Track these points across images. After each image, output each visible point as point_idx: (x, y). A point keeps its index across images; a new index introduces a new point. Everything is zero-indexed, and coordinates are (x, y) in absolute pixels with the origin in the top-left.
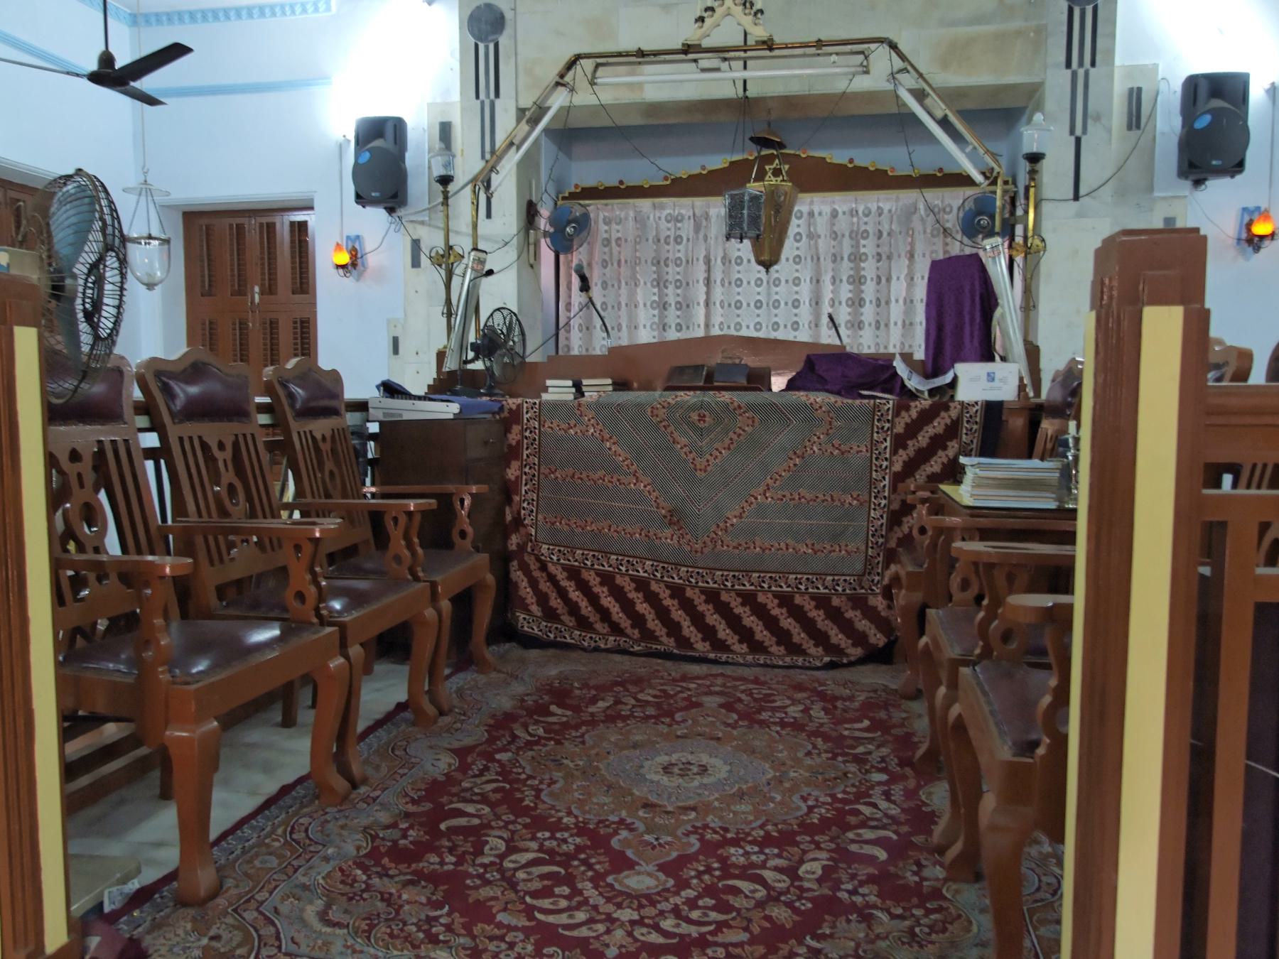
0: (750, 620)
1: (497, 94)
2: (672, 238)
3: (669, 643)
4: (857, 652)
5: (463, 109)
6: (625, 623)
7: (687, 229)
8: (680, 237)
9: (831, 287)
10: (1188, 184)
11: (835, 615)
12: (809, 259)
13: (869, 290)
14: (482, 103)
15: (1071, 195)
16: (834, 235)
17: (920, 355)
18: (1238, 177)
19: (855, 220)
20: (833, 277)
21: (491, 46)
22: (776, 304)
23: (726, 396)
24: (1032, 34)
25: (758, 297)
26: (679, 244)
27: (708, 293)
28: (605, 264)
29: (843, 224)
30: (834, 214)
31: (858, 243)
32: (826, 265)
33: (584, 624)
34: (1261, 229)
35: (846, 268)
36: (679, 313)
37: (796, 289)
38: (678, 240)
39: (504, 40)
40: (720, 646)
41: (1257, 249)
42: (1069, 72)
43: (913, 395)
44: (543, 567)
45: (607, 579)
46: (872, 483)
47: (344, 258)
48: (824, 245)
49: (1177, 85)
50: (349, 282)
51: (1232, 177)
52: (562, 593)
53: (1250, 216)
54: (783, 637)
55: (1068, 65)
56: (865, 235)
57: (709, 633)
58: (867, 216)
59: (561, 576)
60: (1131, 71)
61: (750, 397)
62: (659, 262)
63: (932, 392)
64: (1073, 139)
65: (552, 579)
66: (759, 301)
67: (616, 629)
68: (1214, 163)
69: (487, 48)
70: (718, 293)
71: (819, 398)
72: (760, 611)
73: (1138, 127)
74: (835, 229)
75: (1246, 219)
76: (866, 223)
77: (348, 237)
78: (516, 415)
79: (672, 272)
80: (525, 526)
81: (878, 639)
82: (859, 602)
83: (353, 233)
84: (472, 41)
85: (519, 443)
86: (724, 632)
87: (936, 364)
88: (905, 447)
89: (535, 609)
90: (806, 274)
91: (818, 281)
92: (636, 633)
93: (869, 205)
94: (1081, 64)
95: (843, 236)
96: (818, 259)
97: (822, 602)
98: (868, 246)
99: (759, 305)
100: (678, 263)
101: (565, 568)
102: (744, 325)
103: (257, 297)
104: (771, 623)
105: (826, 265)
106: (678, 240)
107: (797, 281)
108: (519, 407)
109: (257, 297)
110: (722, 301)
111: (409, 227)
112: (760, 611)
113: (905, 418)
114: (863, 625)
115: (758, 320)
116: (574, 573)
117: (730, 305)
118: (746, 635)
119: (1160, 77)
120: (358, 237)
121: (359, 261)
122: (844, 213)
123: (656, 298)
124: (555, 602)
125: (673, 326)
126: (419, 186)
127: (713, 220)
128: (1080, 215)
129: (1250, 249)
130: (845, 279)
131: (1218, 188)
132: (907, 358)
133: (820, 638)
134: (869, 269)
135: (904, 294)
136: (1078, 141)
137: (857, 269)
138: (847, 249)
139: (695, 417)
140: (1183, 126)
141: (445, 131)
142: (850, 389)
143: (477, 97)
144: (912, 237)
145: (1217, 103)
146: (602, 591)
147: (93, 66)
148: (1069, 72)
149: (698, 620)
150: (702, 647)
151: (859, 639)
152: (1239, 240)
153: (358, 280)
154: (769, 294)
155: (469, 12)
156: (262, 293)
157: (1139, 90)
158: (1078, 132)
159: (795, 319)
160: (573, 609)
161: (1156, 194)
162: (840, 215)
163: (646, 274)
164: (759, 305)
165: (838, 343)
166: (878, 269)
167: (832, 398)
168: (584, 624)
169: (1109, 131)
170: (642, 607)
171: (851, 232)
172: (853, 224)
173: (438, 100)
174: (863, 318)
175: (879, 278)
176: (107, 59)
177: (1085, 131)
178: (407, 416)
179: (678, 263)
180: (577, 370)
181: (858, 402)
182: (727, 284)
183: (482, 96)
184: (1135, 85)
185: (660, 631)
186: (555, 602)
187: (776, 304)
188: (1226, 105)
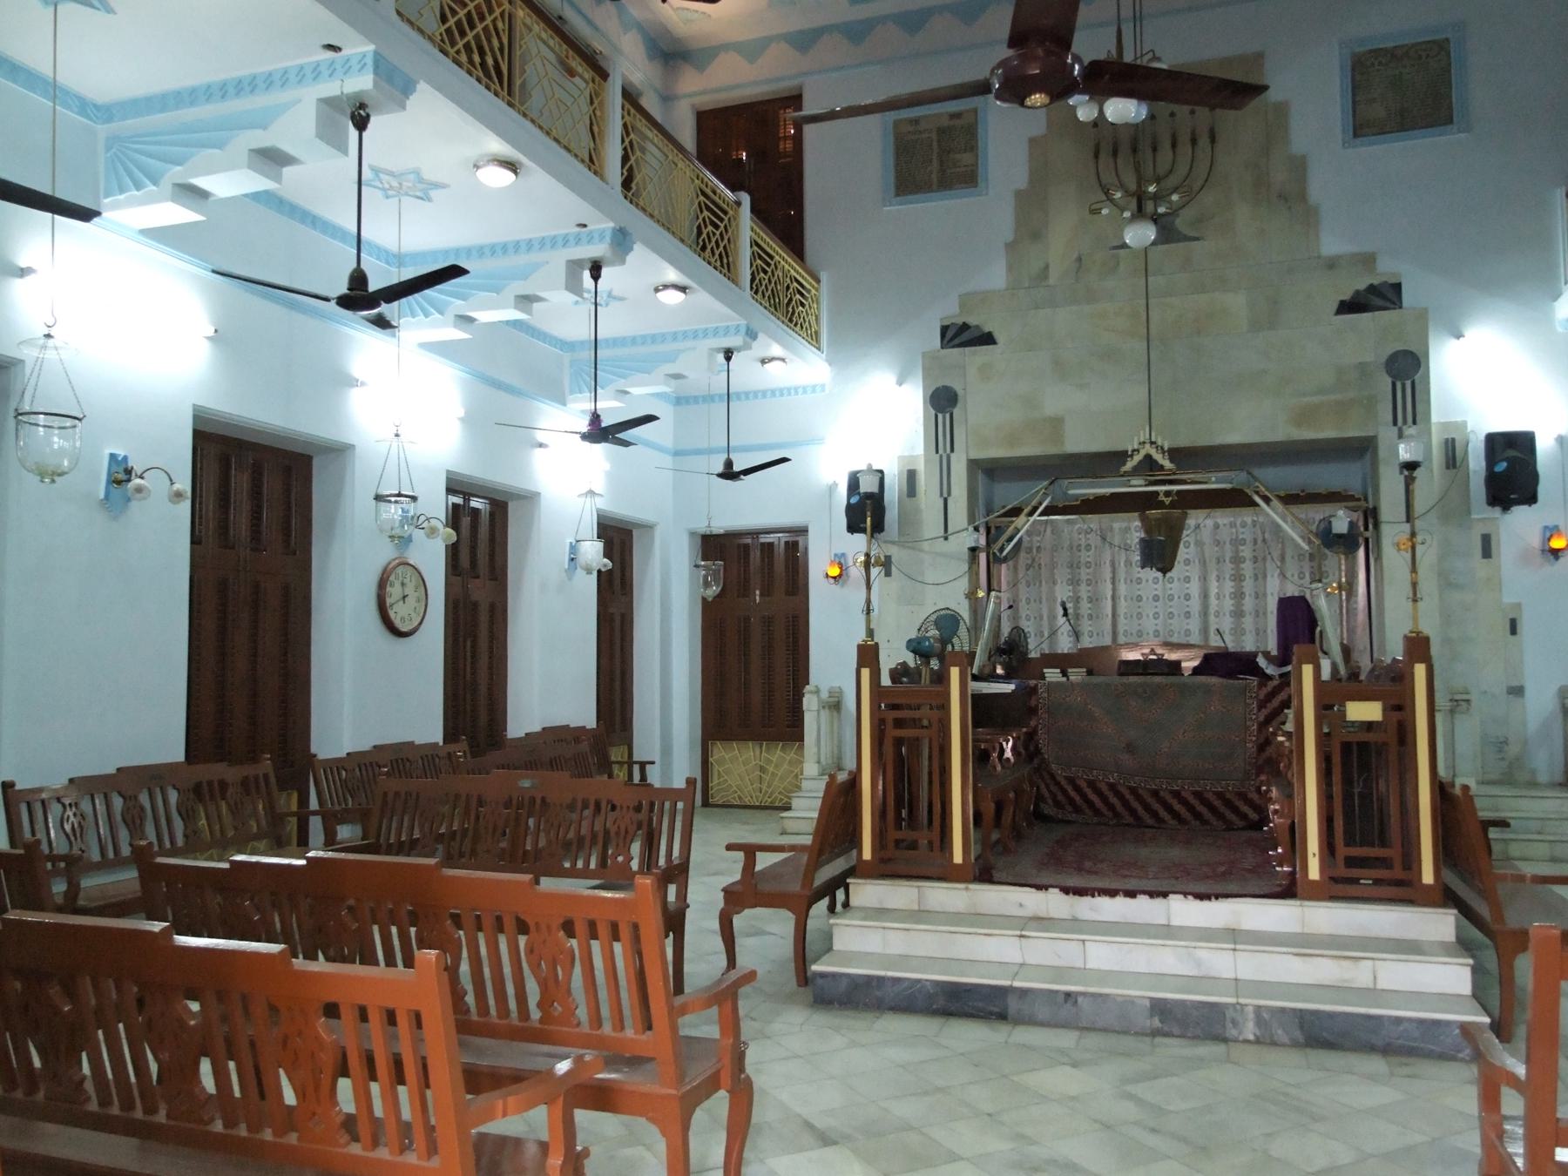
0: (1177, 807)
1: (952, 450)
2: (1083, 547)
3: (1130, 820)
4: (1241, 824)
5: (927, 461)
6: (1104, 810)
7: (1094, 539)
8: (1089, 545)
9: (1217, 584)
10: (1498, 509)
11: (1228, 804)
12: (1197, 561)
13: (1248, 586)
14: (941, 456)
15: (1404, 519)
16: (1218, 543)
17: (1274, 652)
18: (1533, 506)
19: (1234, 530)
20: (1218, 576)
21: (948, 416)
22: (1171, 598)
23: (1157, 679)
24: (1365, 402)
25: (1156, 593)
26: (1088, 551)
27: (1114, 590)
28: (1028, 567)
29: (1225, 535)
30: (1217, 526)
31: (1237, 548)
32: (1212, 566)
33: (1077, 810)
34: (1557, 543)
35: (1228, 568)
36: (1089, 605)
37: (1188, 585)
38: (1088, 547)
39: (956, 411)
40: (1160, 820)
41: (1557, 558)
42: (1396, 429)
43: (1270, 678)
44: (1053, 777)
45: (1091, 784)
46: (1247, 728)
47: (835, 571)
48: (1210, 551)
49: (1482, 437)
50: (835, 588)
52: (1064, 792)
53: (1551, 532)
54: (1198, 816)
55: (1395, 423)
56: (1244, 541)
57: (1155, 814)
58: (1244, 527)
59: (1064, 782)
60: (1445, 426)
61: (1171, 679)
62: (1072, 566)
63: (1281, 676)
65: (1058, 784)
66: (1156, 595)
67: (1097, 812)
68: (1512, 496)
69: (944, 418)
70: (1123, 589)
71: (1214, 680)
72: (1184, 802)
73: (1454, 466)
74: (1217, 537)
75: (1548, 534)
76: (1243, 533)
77: (836, 555)
78: (1034, 690)
79: (1084, 574)
80: (1042, 754)
81: (1253, 816)
82: (1243, 796)
83: (839, 552)
84: (933, 412)
85: (1037, 706)
86: (1163, 813)
87: (1283, 658)
88: (1265, 707)
89: (1050, 801)
90: (1194, 572)
91: (1205, 579)
92: (1110, 814)
93: (1245, 519)
94: (1405, 422)
95: (1225, 543)
96: (1205, 561)
97: (1220, 795)
98: (1246, 552)
99: (1156, 599)
100: (1088, 565)
101: (1066, 778)
102: (1144, 614)
103: (758, 598)
104: (1191, 809)
105: (1212, 566)
106: (1088, 547)
107: (1187, 580)
108: (1036, 685)
109: (758, 598)
110: (1125, 596)
111: (883, 545)
112: (1184, 802)
113: (1264, 692)
114: (1245, 809)
115: (1157, 610)
116: (1071, 781)
117: (1132, 599)
118: (1176, 815)
119: (1469, 430)
120: (843, 555)
121: (844, 572)
122: (1225, 525)
123: (1071, 594)
124: (1060, 797)
125: (1086, 616)
126: (891, 515)
127: (1117, 531)
129: (1552, 557)
130: (1228, 576)
131: (1520, 513)
132: (1267, 655)
133: (1221, 817)
134: (1248, 568)
135: (1277, 589)
137: (1238, 569)
138: (1228, 555)
139: (1140, 690)
140: (1487, 469)
141: (911, 476)
142: (1230, 674)
143: (937, 452)
144: (1282, 543)
145: (1511, 453)
146: (1089, 792)
147: (720, 468)
148: (1396, 429)
149: (1147, 807)
150: (1150, 821)
151: (1244, 817)
152: (1543, 551)
153: (842, 586)
154: (1164, 589)
155: (930, 393)
156: (761, 595)
157: (1453, 440)
159: (1187, 609)
160: (1071, 801)
161: (1473, 517)
162: (1221, 527)
163: (1062, 574)
164: (1156, 599)
165: (1223, 645)
166: (1255, 569)
167: (1221, 680)
168: (1077, 810)
169: (1432, 471)
170: (1114, 800)
171: (1232, 540)
172: (1232, 533)
173: (906, 454)
174: (1244, 608)
175: (1256, 575)
176: (729, 464)
178: (985, 691)
179: (1088, 565)
180: (1063, 662)
181: (1236, 682)
182: (1129, 582)
183: (941, 451)
184: (1450, 437)
185: (1125, 813)
186: (1060, 797)
187: (1171, 598)
188: (1519, 455)
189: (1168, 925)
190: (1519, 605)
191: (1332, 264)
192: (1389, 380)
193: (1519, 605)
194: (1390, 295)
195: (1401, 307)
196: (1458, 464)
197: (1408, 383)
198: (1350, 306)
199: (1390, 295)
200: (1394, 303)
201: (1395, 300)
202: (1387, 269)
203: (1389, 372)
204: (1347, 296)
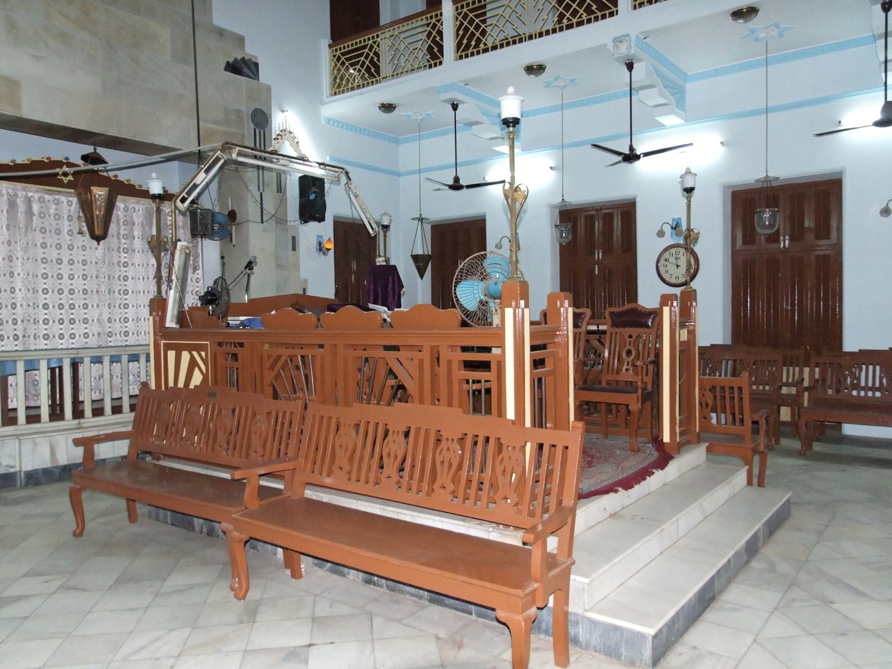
18: (322, 223)
51: (319, 222)
64: (259, 192)
73: (281, 192)
128: (264, 230)
131: (313, 225)
136: (261, 194)
158: (261, 191)
177: (263, 191)
189: (650, 493)
190: (306, 281)
191: (221, 33)
192: (253, 126)
193: (306, 281)
194: (253, 68)
195: (258, 80)
196: (282, 192)
197: (262, 131)
198: (235, 68)
199: (253, 68)
200: (255, 76)
201: (256, 74)
202: (251, 50)
203: (253, 123)
204: (231, 61)
